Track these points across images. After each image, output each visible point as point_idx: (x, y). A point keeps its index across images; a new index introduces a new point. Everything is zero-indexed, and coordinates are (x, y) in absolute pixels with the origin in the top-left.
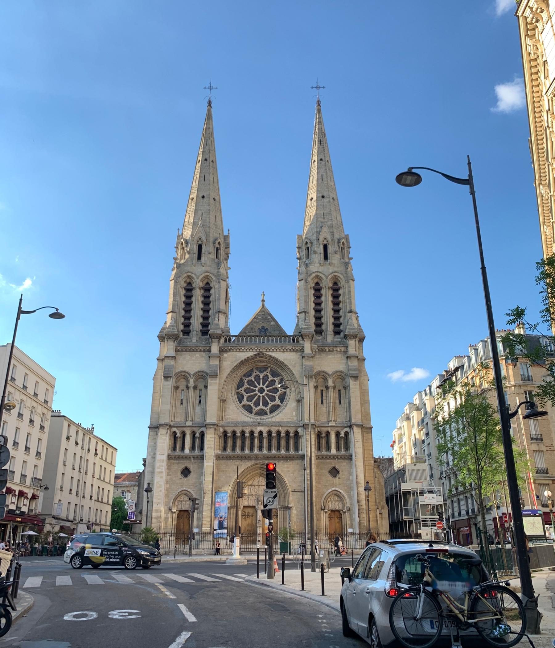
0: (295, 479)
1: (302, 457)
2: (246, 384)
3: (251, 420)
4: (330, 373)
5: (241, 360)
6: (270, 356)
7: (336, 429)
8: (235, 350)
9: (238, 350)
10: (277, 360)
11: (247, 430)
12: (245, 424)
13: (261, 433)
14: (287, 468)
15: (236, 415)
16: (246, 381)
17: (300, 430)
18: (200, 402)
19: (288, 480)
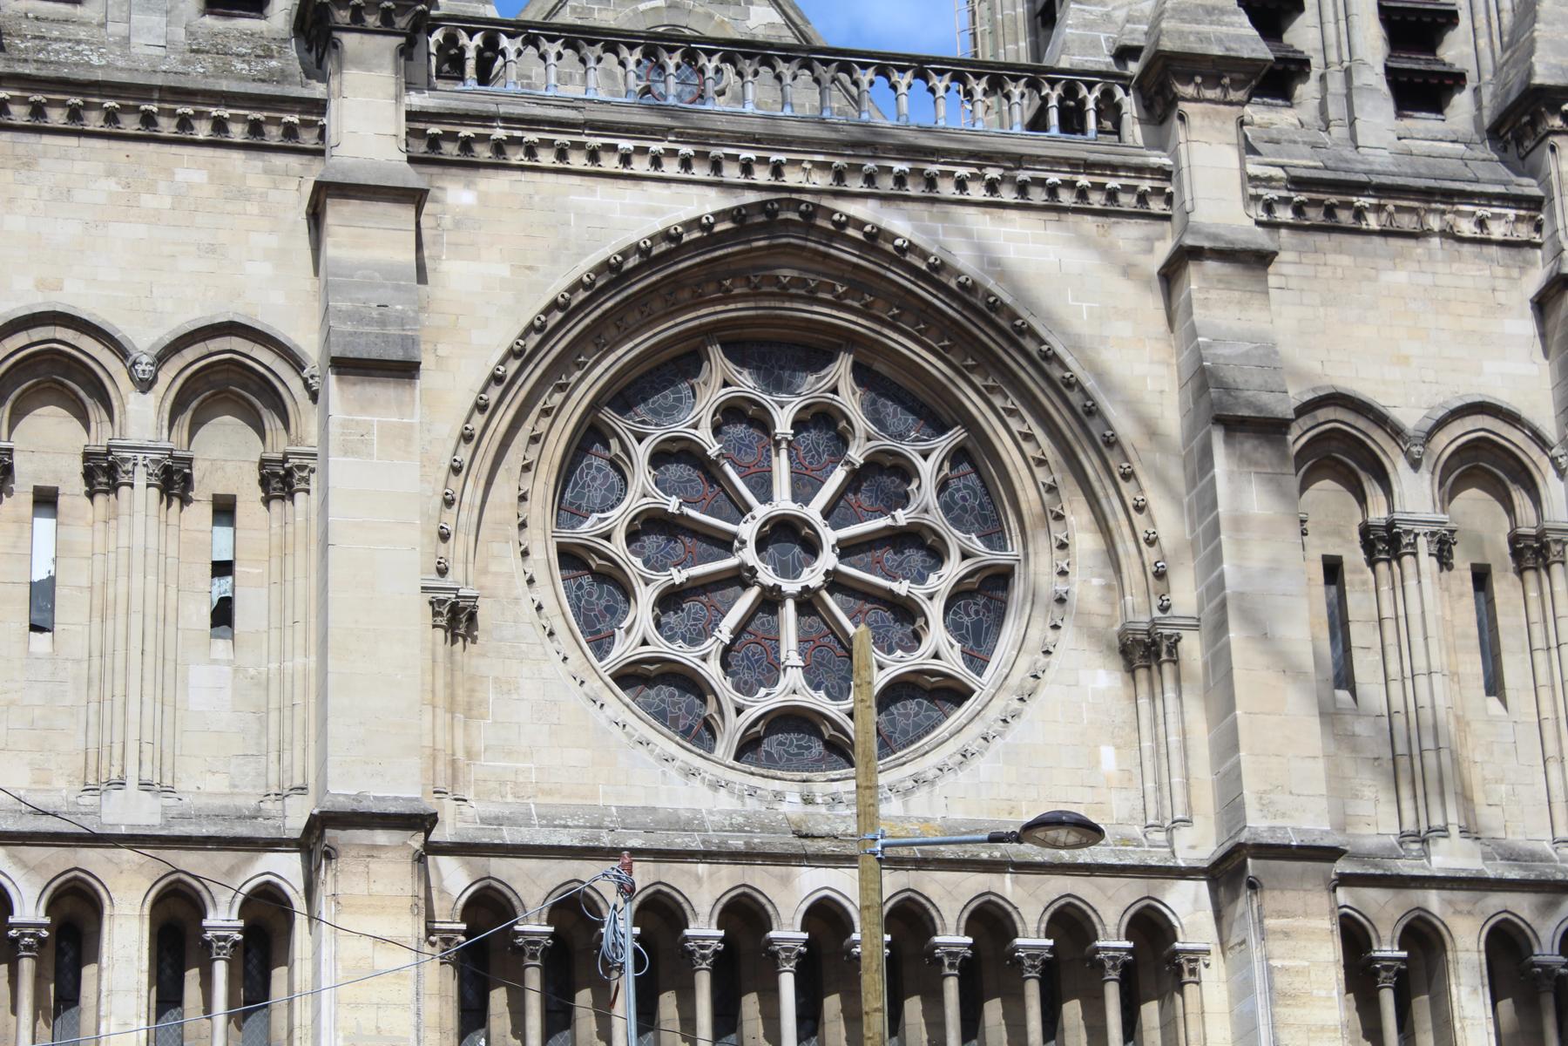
2: (642, 476)
3: (725, 802)
4: (1411, 417)
5: (607, 250)
6: (875, 239)
7: (1497, 902)
8: (546, 158)
9: (577, 161)
10: (935, 273)
11: (703, 893)
12: (680, 841)
13: (825, 916)
15: (569, 758)
16: (642, 452)
17: (1189, 908)
18: (223, 614)
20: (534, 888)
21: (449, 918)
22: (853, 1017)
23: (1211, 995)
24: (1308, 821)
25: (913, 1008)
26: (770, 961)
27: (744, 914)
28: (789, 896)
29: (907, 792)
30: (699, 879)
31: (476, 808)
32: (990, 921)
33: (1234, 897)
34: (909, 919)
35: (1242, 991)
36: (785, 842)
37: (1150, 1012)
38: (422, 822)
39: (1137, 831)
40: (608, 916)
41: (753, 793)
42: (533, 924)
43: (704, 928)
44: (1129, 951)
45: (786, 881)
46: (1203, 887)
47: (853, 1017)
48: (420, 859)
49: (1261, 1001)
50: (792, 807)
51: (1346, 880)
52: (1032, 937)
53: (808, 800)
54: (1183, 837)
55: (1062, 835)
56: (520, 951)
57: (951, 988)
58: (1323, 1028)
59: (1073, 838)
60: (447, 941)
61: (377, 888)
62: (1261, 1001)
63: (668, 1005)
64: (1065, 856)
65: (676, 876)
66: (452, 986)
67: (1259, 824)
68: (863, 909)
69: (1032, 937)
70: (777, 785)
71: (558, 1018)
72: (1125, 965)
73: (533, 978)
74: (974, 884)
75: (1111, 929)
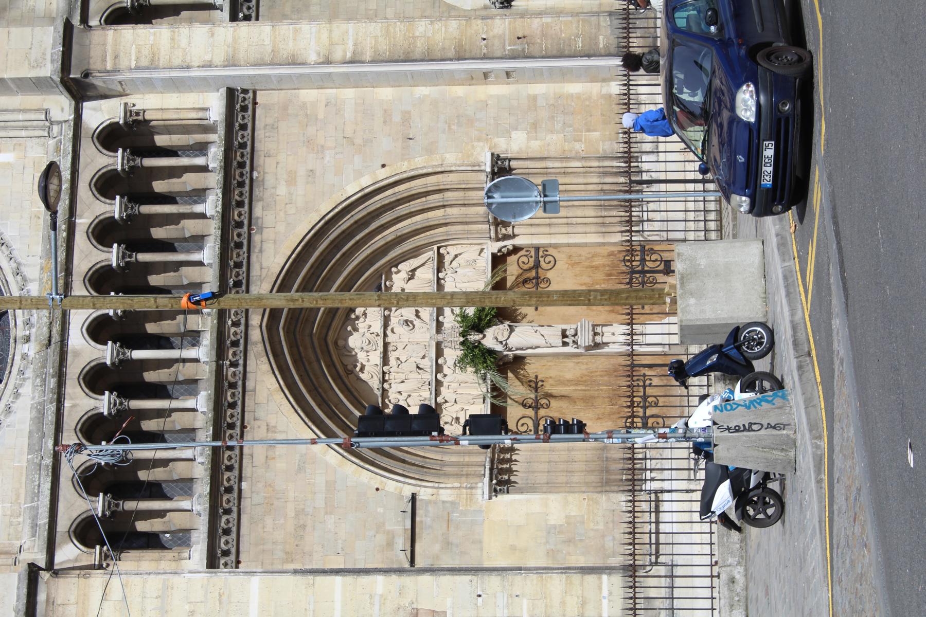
0: (350, 140)
1: (239, 103)
3: (27, 390)
11: (82, 403)
12: (50, 417)
13: (99, 330)
14: (292, 180)
17: (98, 115)
19: (359, 174)
20: (76, 505)
21: (93, 555)
22: (159, 316)
23: (152, 104)
24: (48, 39)
25: (155, 280)
26: (124, 364)
27: (96, 379)
28: (85, 352)
29: (24, 279)
30: (74, 406)
31: (26, 540)
32: (104, 233)
33: (94, 86)
34: (101, 280)
35: (149, 85)
36: (53, 354)
37: (161, 140)
38: (33, 572)
39: (52, 142)
40: (95, 460)
41: (21, 372)
42: (98, 505)
43: (104, 403)
44: (124, 151)
45: (77, 354)
46: (87, 105)
47: (159, 316)
48: (56, 573)
49: (155, 75)
50: (31, 349)
51: (84, 19)
52: (115, 208)
53: (27, 339)
54: (56, 115)
55: (53, 187)
56: (114, 513)
57: (143, 257)
58: (173, 39)
59: (55, 181)
60: (107, 557)
61: (73, 599)
62: (155, 75)
63: (149, 425)
64: (66, 186)
65: (71, 420)
66: (133, 554)
67: (49, 69)
68: (94, 307)
69: (115, 208)
70: (18, 358)
71: (155, 491)
72: (132, 153)
73: (130, 505)
74: (81, 241)
75: (111, 161)
